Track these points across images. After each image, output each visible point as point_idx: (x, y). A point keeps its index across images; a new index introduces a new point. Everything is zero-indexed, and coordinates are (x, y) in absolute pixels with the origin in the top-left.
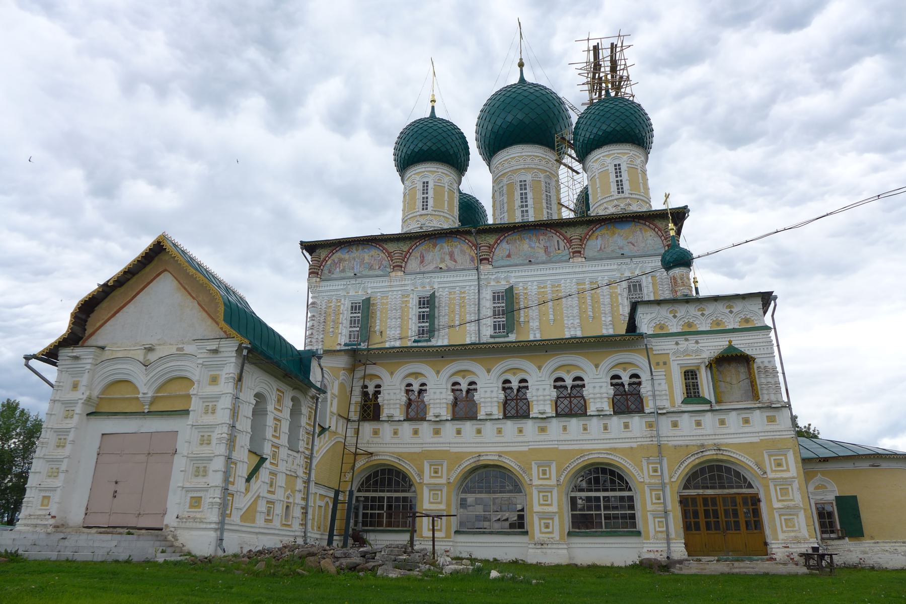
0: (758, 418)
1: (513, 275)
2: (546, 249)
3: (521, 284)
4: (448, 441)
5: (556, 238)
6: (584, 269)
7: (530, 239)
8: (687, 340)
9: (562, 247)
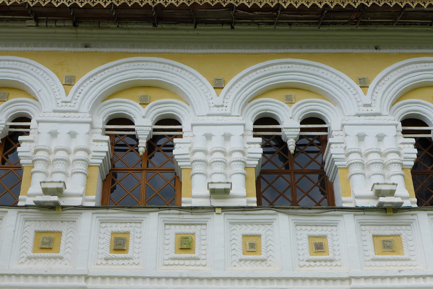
4: (81, 269)
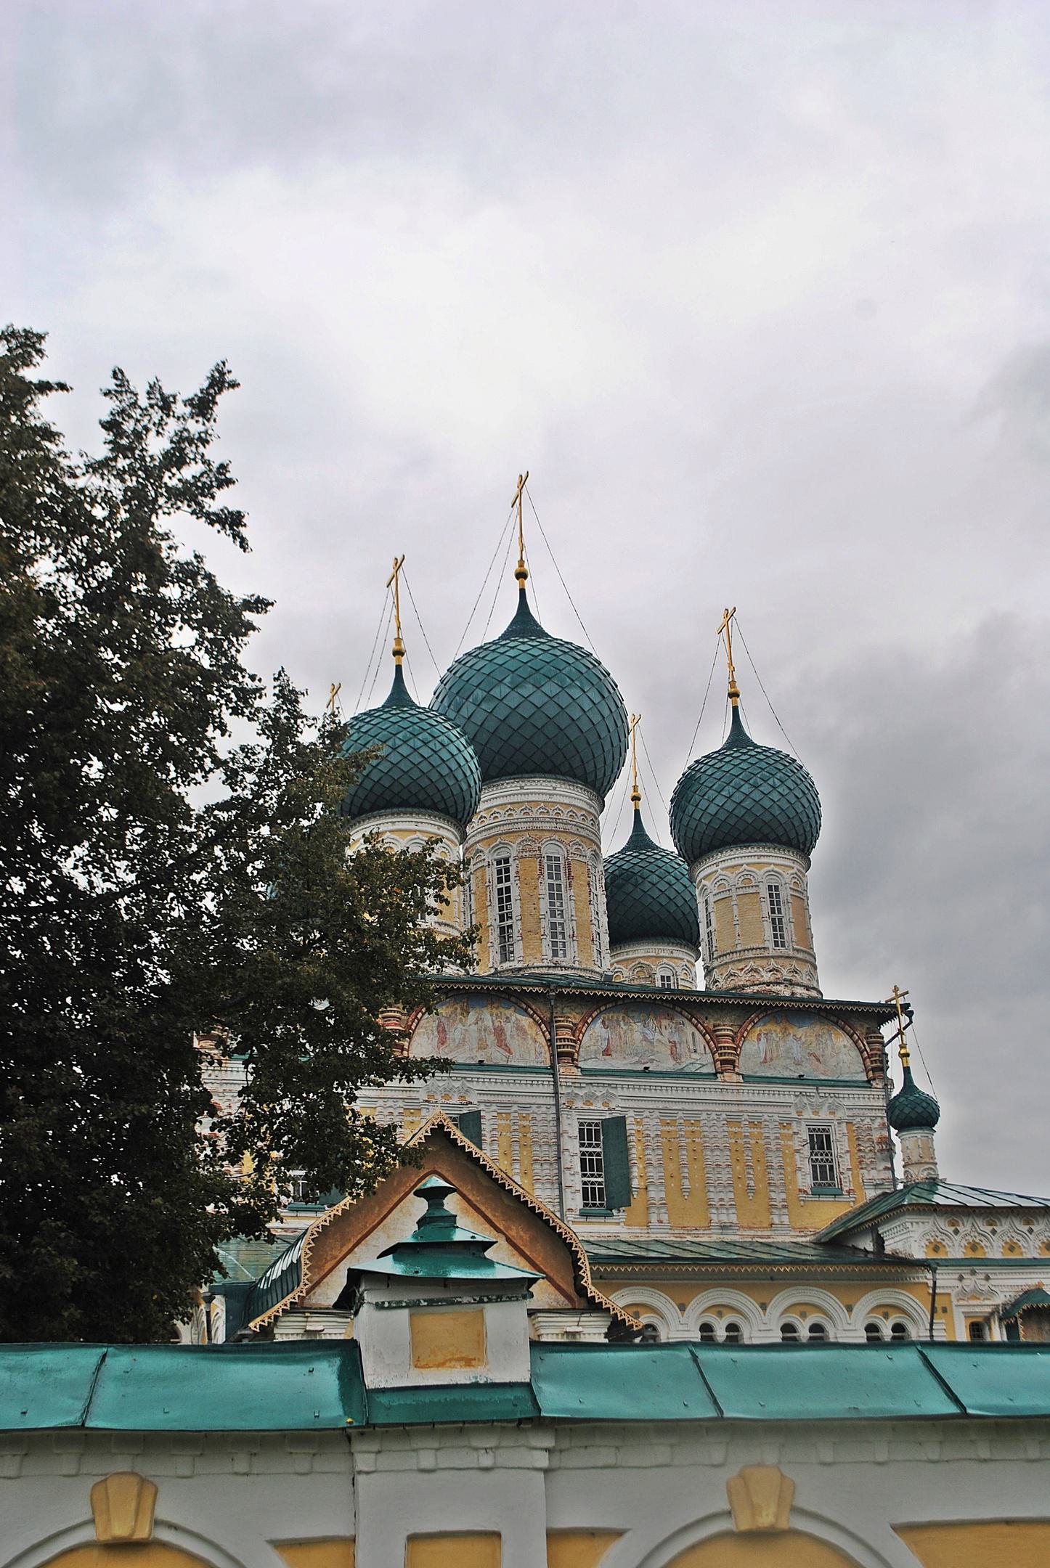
1: (620, 1092)
5: (689, 1029)
8: (973, 1273)
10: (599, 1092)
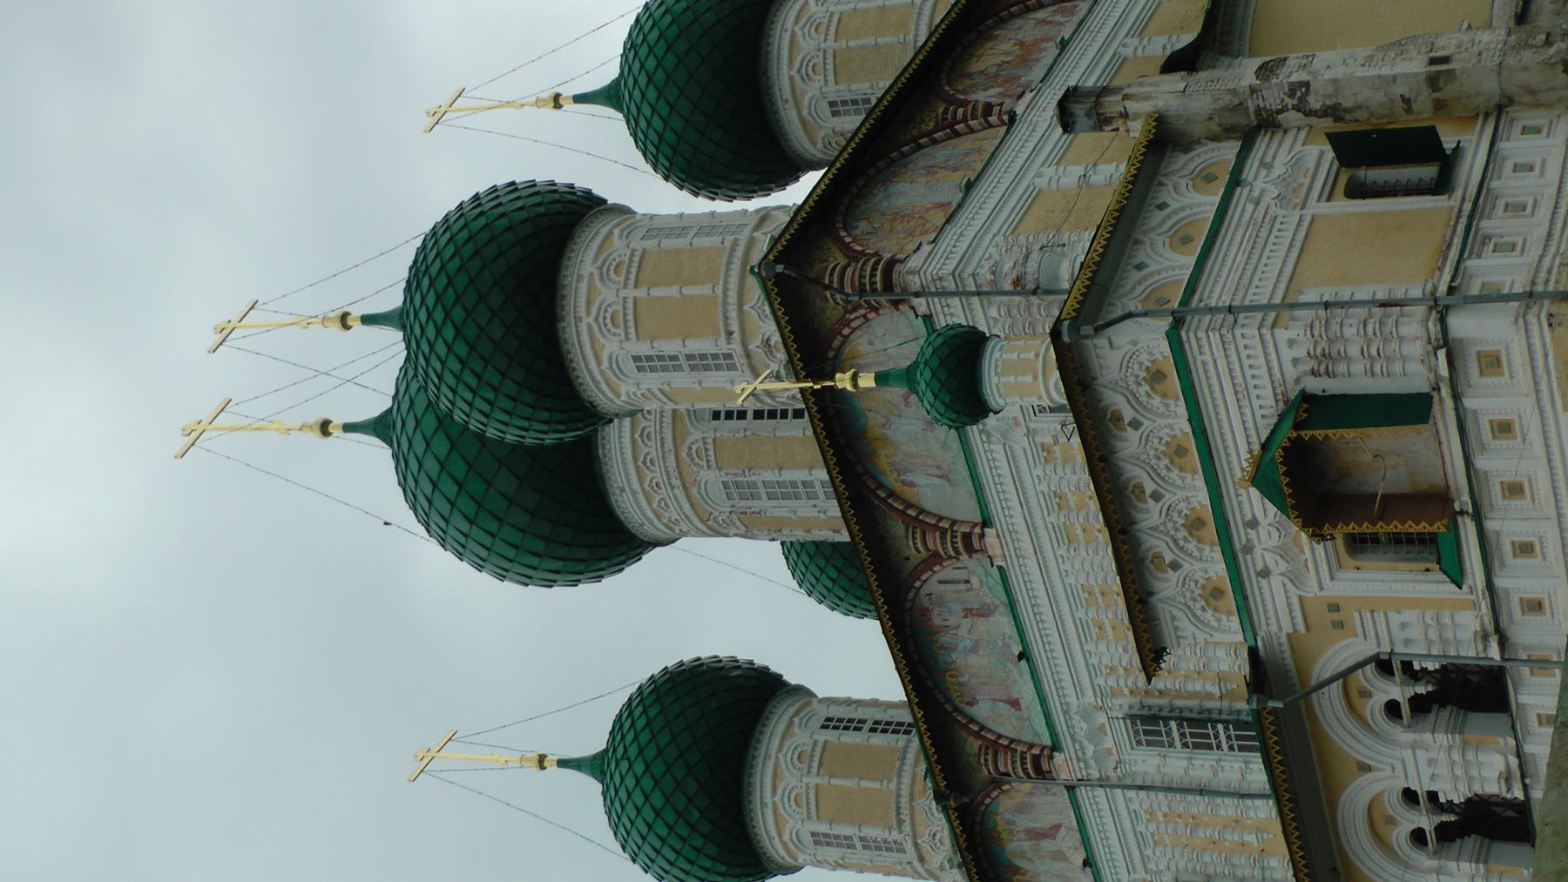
0: (1485, 400)
1: (1073, 700)
2: (968, 612)
3: (1100, 681)
6: (1022, 528)
7: (950, 648)
8: (1248, 549)
9: (961, 574)
10: (1081, 727)
